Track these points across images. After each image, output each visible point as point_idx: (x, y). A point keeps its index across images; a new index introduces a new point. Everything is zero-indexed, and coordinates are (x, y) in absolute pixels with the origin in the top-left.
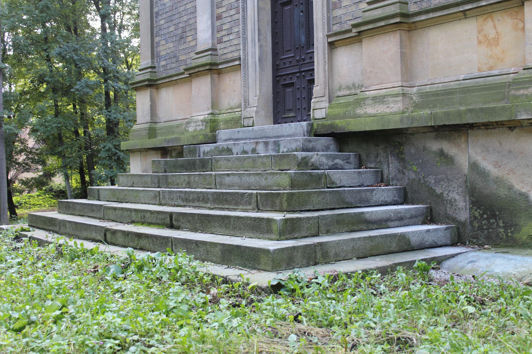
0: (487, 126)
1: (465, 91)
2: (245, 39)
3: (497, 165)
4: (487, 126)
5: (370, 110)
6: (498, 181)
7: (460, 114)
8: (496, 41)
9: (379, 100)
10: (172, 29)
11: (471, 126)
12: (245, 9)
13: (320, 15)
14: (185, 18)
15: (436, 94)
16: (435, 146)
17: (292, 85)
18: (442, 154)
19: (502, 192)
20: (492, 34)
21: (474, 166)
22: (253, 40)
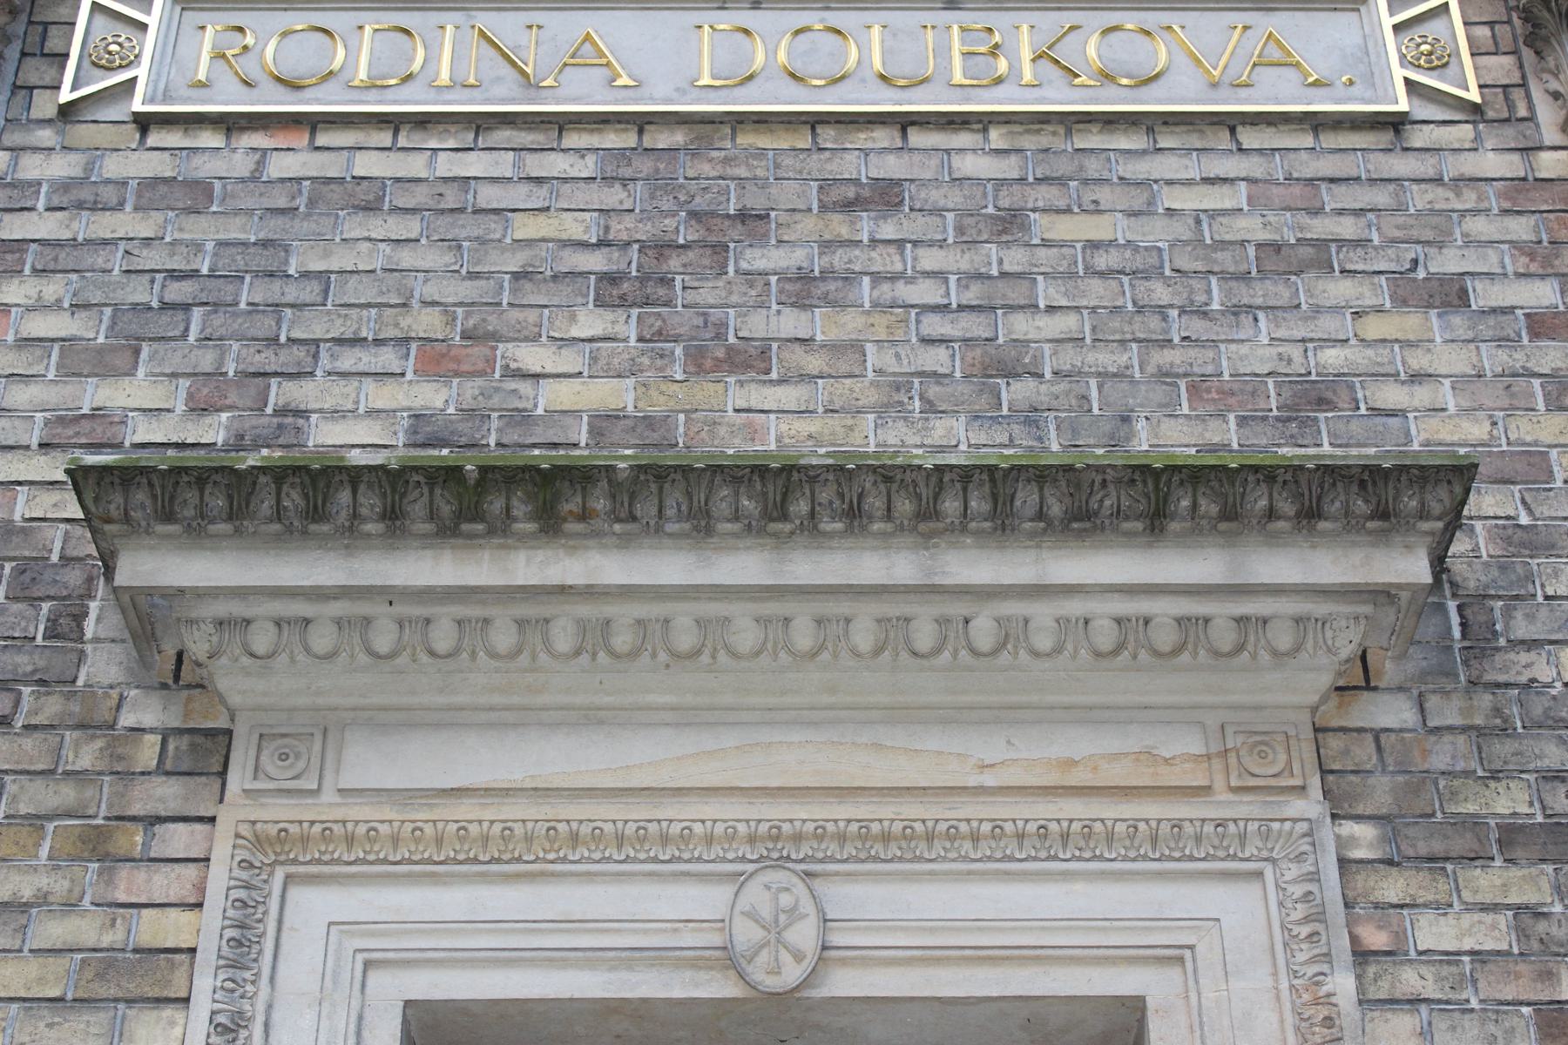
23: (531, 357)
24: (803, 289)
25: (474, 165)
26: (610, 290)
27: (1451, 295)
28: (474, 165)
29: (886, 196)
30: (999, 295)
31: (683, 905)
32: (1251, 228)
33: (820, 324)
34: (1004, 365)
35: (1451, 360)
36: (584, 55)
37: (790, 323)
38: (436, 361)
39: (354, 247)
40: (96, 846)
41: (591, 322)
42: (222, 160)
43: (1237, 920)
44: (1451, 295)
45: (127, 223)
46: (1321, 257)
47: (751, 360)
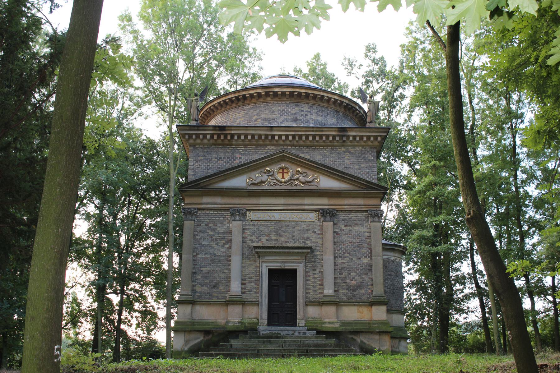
0: (366, 332)
1: (356, 323)
2: (262, 295)
3: (368, 341)
4: (366, 332)
5: (328, 326)
6: (368, 345)
7: (360, 329)
8: (362, 313)
9: (329, 323)
10: (207, 281)
11: (362, 332)
12: (262, 285)
13: (301, 295)
14: (218, 280)
15: (347, 323)
16: (350, 336)
17: (278, 314)
18: (352, 338)
19: (369, 347)
20: (361, 311)
21: (362, 341)
22: (265, 296)
23: (271, 236)
24: (284, 232)
25: (268, 223)
26: (275, 232)
27: (315, 232)
28: (268, 223)
29: (288, 226)
30: (294, 232)
31: (279, 264)
32: (306, 228)
33: (285, 234)
34: (293, 236)
35: (314, 236)
36: (273, 216)
37: (283, 234)
38: (267, 236)
39: (263, 229)
40: (255, 261)
41: (274, 234)
42: (256, 223)
43: (301, 265)
44: (315, 232)
45: (251, 227)
46: (309, 230)
47: (281, 236)
